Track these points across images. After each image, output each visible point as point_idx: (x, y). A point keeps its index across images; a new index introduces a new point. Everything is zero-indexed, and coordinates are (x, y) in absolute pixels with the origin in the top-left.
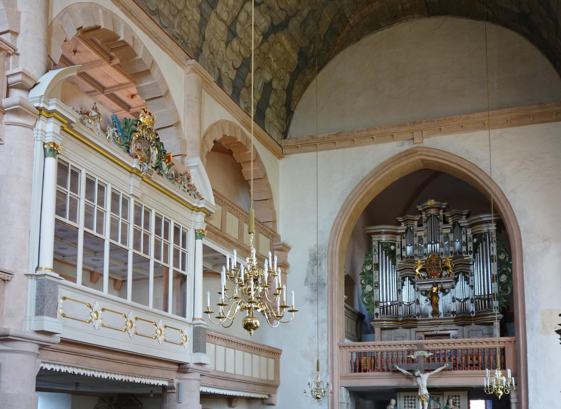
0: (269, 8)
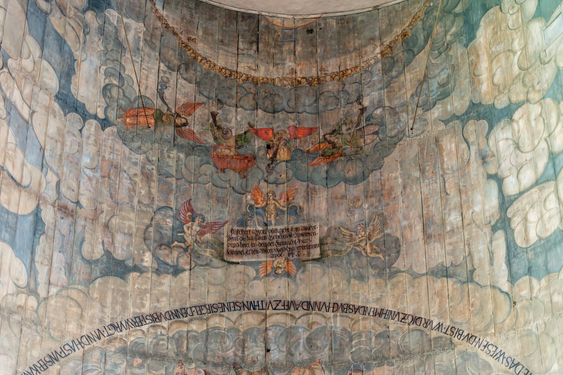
0: (484, 159)
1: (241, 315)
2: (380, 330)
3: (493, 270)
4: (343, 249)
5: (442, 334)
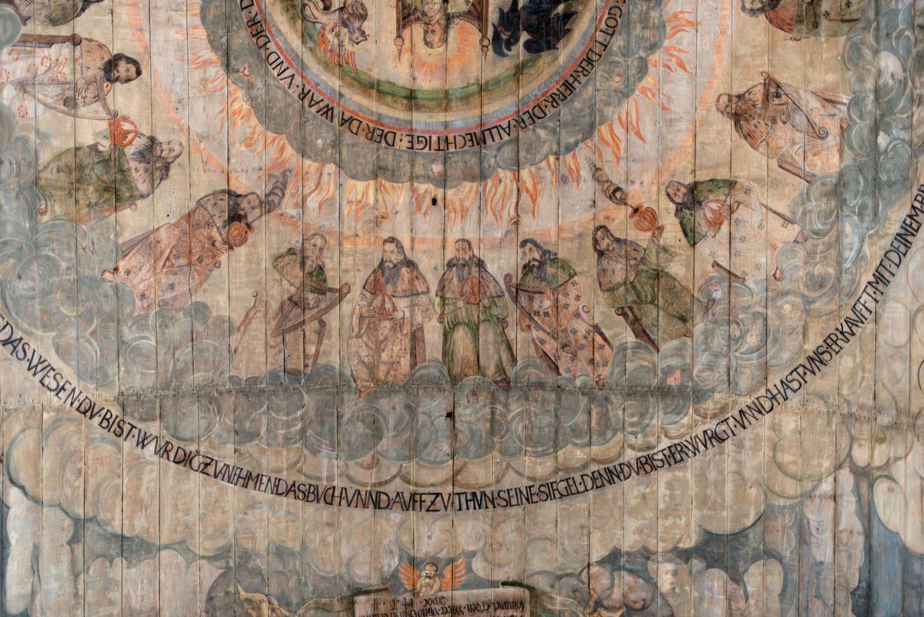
1: (498, 482)
2: (250, 447)
3: (34, 534)
4: (312, 612)
5: (140, 425)
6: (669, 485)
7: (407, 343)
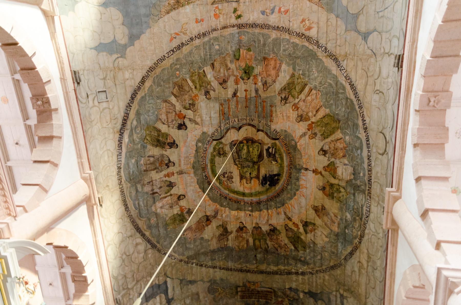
2: (215, 261)
6: (302, 279)
7: (245, 242)
